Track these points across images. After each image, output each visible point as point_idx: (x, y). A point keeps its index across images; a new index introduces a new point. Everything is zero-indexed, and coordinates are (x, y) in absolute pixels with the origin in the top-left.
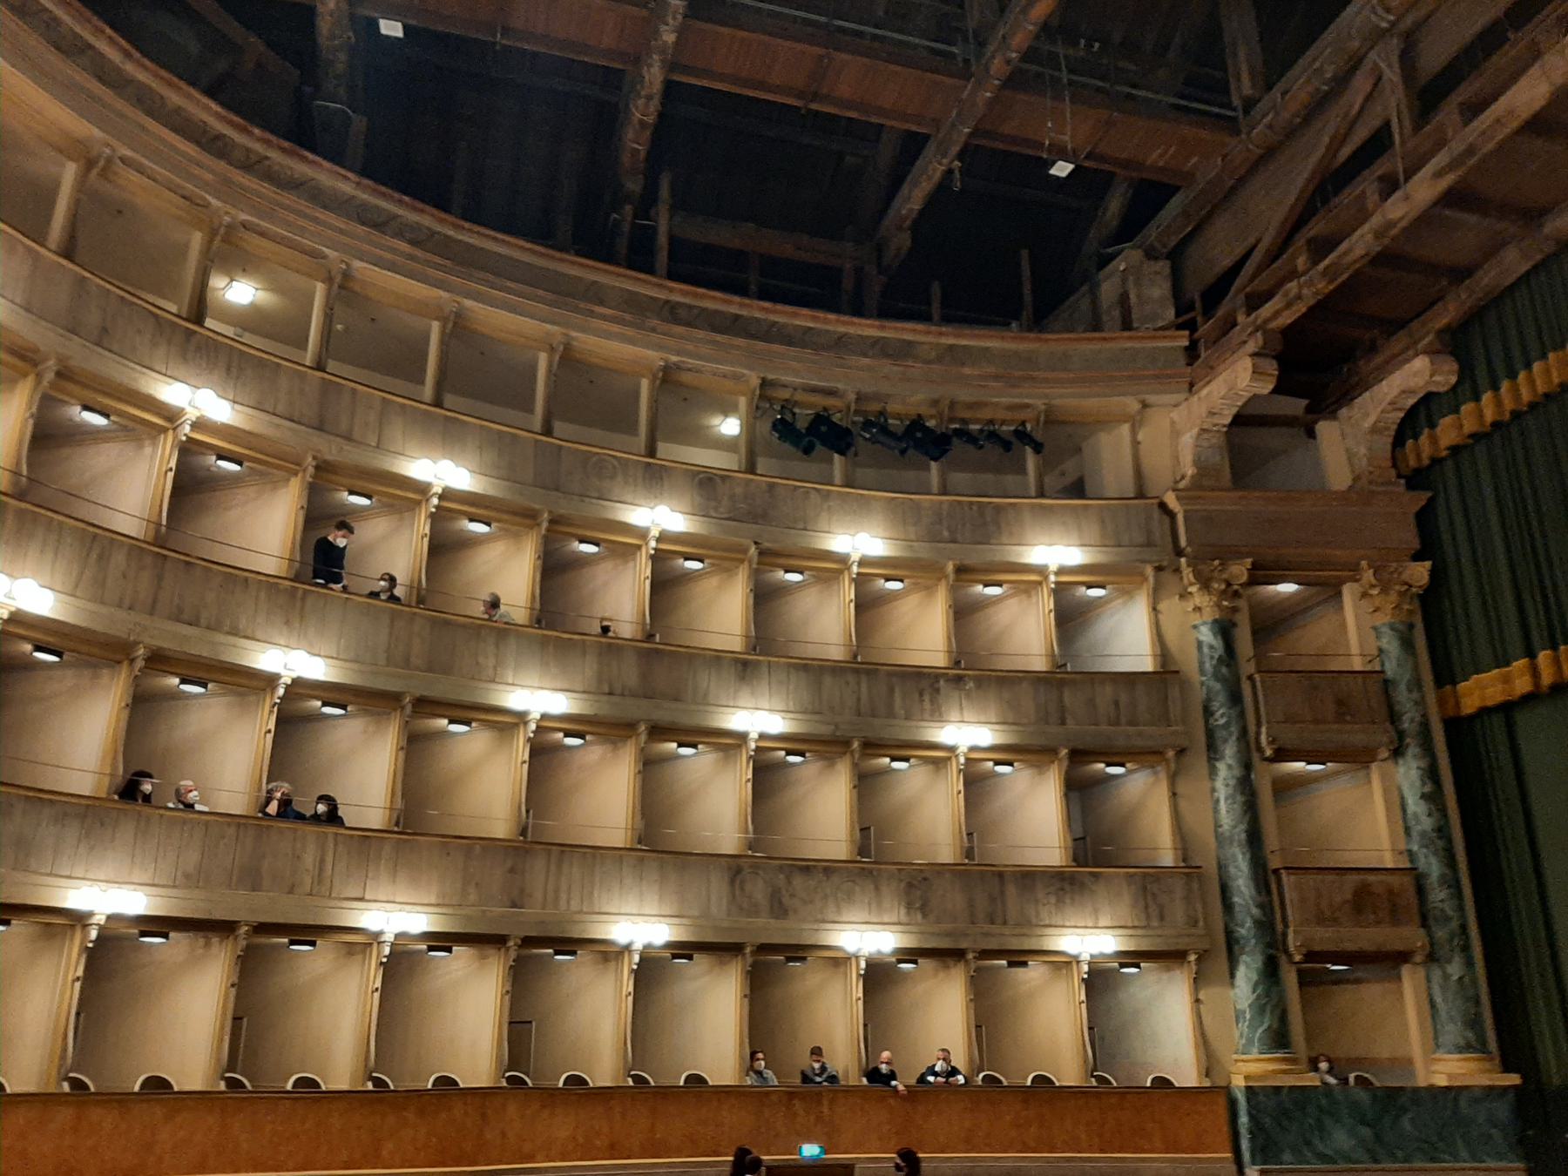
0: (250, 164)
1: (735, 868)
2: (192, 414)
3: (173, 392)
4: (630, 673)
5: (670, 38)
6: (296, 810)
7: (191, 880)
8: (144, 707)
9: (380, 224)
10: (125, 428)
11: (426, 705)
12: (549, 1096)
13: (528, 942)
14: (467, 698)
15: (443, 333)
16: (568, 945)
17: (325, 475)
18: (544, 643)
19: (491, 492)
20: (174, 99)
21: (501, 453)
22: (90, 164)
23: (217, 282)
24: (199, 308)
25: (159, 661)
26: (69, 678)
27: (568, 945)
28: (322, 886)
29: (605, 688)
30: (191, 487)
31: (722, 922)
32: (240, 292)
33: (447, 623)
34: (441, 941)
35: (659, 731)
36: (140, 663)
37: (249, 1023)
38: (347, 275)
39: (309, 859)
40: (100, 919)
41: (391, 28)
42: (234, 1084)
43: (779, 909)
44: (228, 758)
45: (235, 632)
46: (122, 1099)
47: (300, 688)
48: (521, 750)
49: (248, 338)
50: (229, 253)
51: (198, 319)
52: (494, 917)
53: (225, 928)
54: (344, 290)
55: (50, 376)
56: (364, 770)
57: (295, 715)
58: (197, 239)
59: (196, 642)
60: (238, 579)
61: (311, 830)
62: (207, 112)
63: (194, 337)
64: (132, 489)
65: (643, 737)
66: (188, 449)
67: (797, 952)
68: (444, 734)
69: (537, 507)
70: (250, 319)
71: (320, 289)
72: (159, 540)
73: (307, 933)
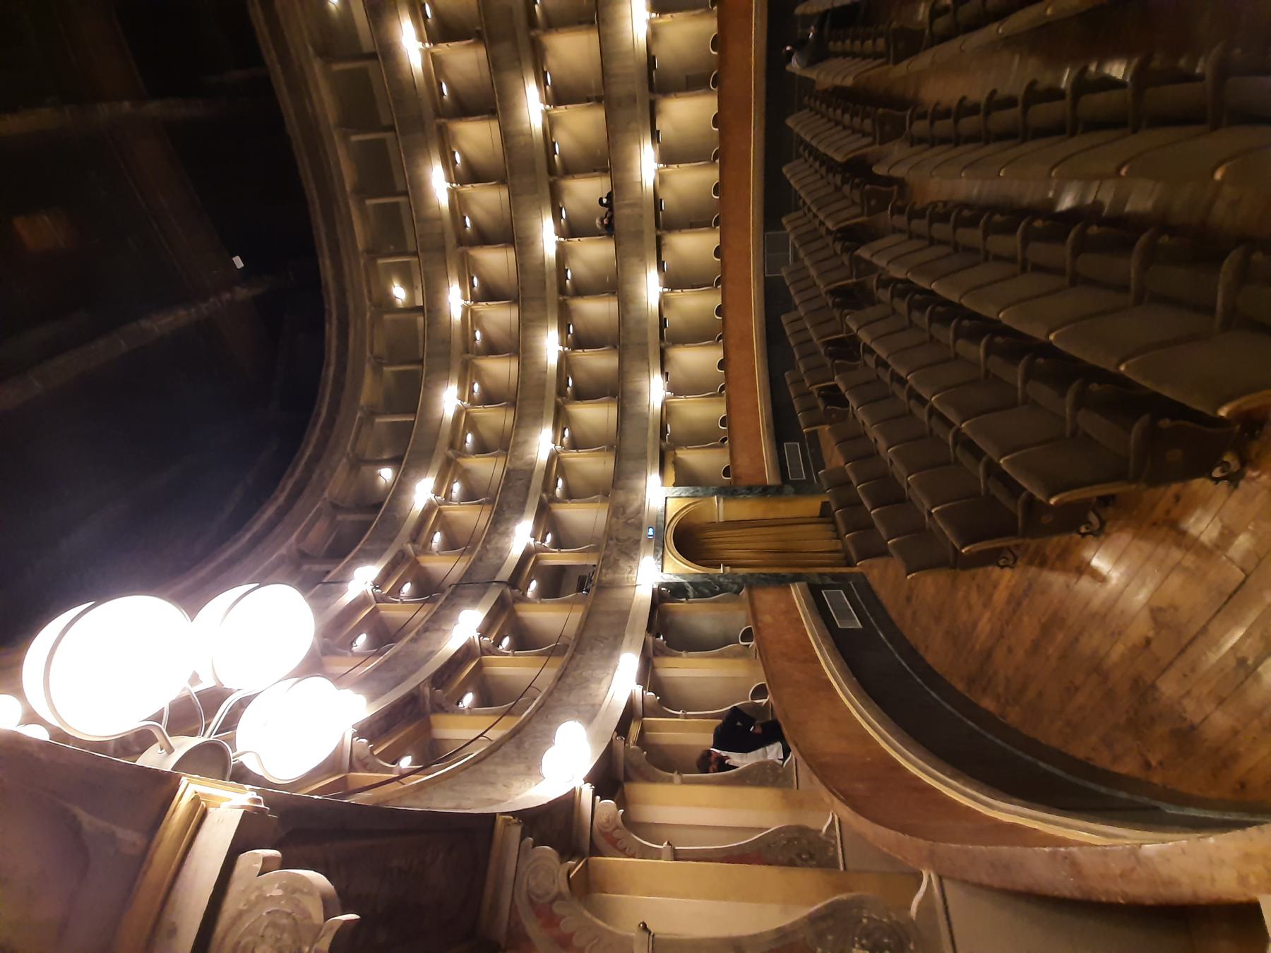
0: (342, 306)
2: (462, 302)
4: (504, 48)
5: (126, 105)
6: (608, 221)
7: (643, 260)
8: (582, 290)
11: (551, 169)
14: (542, 149)
15: (371, 197)
16: (651, 59)
18: (504, 110)
19: (438, 156)
20: (334, 343)
21: (415, 154)
22: (381, 365)
25: (562, 290)
26: (576, 319)
27: (651, 59)
28: (638, 204)
29: (517, 66)
30: (490, 293)
32: (399, 293)
33: (510, 166)
34: (655, 135)
38: (368, 251)
39: (627, 211)
41: (239, 262)
42: (717, 223)
44: (593, 253)
45: (543, 264)
46: (723, 266)
47: (560, 233)
48: (561, 111)
50: (387, 302)
51: (420, 309)
52: (641, 110)
53: (659, 240)
54: (374, 252)
56: (585, 191)
57: (571, 230)
58: (387, 317)
59: (552, 280)
61: (616, 213)
62: (331, 329)
63: (431, 307)
64: (499, 316)
65: (538, 32)
66: (475, 299)
68: (560, 155)
69: (435, 127)
70: (408, 283)
73: (657, 202)
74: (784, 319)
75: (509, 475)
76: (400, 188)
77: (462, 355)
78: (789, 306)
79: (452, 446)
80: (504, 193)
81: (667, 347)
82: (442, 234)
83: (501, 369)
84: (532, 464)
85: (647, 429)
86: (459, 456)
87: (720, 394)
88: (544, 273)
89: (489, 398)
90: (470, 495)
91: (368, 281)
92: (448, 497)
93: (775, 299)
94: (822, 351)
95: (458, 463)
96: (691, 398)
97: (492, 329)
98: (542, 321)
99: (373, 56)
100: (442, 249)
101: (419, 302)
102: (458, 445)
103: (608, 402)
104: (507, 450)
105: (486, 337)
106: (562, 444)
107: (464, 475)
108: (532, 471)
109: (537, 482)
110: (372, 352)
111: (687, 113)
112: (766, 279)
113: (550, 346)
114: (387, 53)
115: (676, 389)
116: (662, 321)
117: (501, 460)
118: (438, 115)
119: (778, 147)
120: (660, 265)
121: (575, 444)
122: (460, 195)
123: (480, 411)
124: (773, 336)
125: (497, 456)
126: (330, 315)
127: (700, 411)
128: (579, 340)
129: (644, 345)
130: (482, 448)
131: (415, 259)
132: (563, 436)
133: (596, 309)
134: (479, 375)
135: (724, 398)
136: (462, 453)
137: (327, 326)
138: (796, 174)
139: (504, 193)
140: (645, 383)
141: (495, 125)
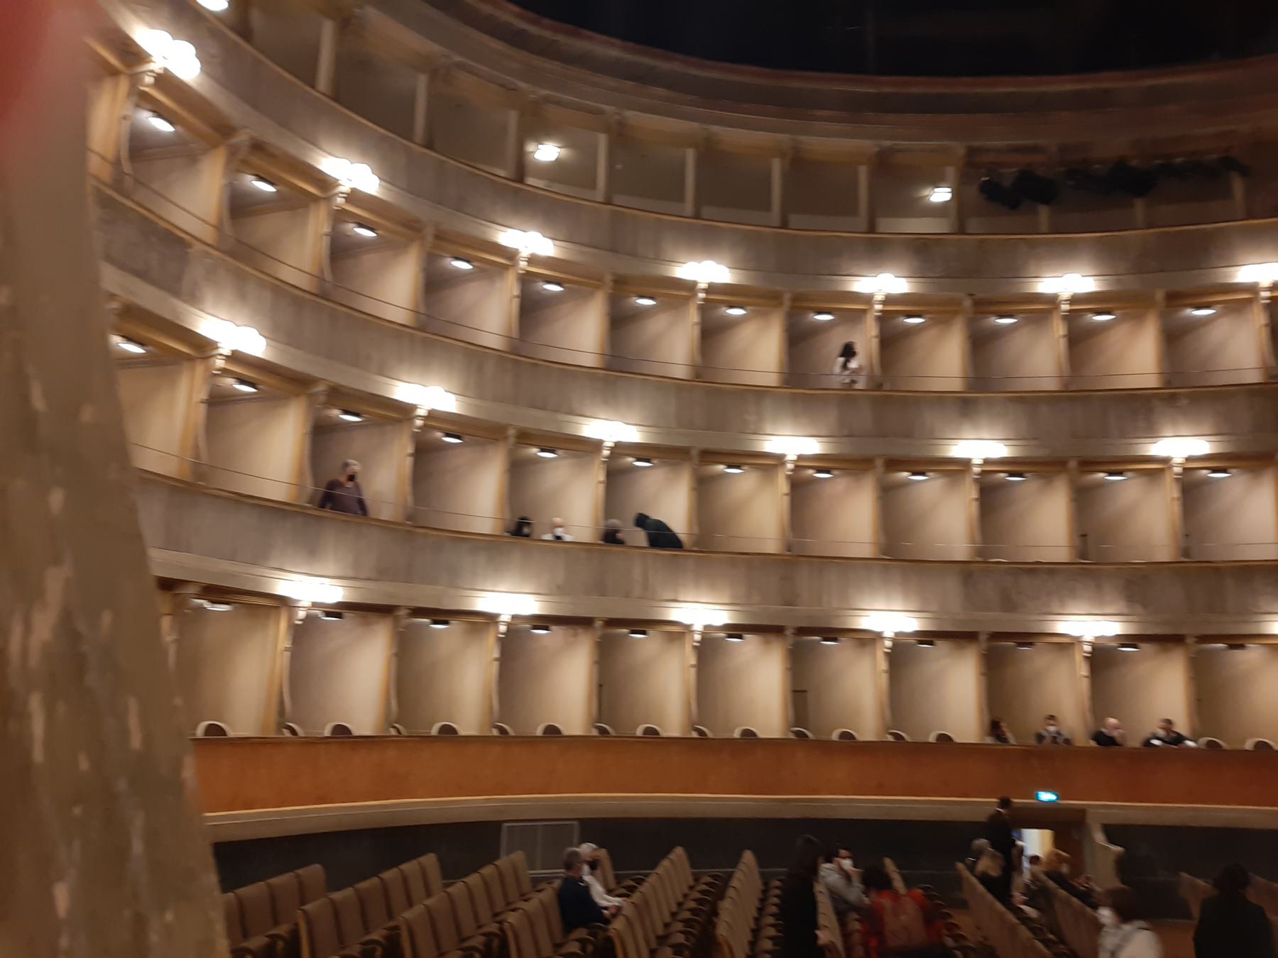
1: (967, 572)
3: (507, 237)
7: (559, 590)
8: (518, 471)
9: (642, 77)
10: (482, 270)
11: (709, 456)
12: (825, 747)
13: (802, 631)
16: (832, 633)
17: (621, 287)
18: (794, 398)
21: (751, 252)
23: (530, 147)
24: (522, 167)
25: (525, 437)
27: (832, 633)
28: (648, 594)
31: (958, 615)
32: (547, 152)
34: (735, 631)
35: (894, 464)
36: (512, 440)
37: (609, 687)
38: (622, 124)
39: (637, 572)
40: (505, 618)
42: (603, 731)
43: (1009, 604)
44: (576, 505)
47: (620, 449)
48: (782, 485)
49: (556, 187)
51: (520, 178)
52: (772, 613)
54: (621, 137)
55: (430, 239)
58: (513, 117)
60: (570, 373)
63: (523, 194)
64: (491, 314)
66: (527, 279)
67: (1027, 639)
68: (724, 476)
70: (555, 171)
71: (602, 140)
72: (514, 350)
73: (641, 625)
74: (430, 860)
75: (175, 242)
76: (706, 211)
77: (433, 224)
78: (452, 872)
79: (258, 147)
80: (680, 372)
81: (397, 619)
82: (634, 254)
83: (396, 289)
84: (194, 299)
85: (232, 558)
86: (233, 152)
87: (282, 725)
88: (557, 411)
89: (341, 251)
90: (140, 147)
91: (579, 108)
92: (144, 100)
93: (467, 843)
94: (375, 936)
95: (215, 146)
96: (283, 660)
97: (470, 294)
98: (473, 387)
99: (872, 229)
100: (613, 250)
101: (530, 181)
102: (255, 160)
103: (299, 486)
104: (233, 254)
105: (458, 279)
106: (225, 372)
107: (181, 154)
108: (176, 293)
109: (148, 297)
110: (459, 66)
111: (761, 689)
112: (497, 825)
113: (429, 393)
114: (876, 250)
115: (306, 632)
116: (441, 616)
117: (208, 234)
118: (796, 299)
119: (711, 840)
120: (542, 621)
121: (218, 401)
122: (686, 300)
123: (317, 226)
124: (396, 841)
125: (218, 228)
126: (533, 22)
127: (248, 685)
128: (431, 446)
129: (408, 575)
130: (240, 207)
131: (599, 195)
132: (242, 381)
133: (481, 496)
134: (389, 246)
135: (272, 734)
136: (238, 164)
137: (516, 9)
138: (673, 874)
139: (680, 372)
140: (331, 568)
141: (771, 379)
